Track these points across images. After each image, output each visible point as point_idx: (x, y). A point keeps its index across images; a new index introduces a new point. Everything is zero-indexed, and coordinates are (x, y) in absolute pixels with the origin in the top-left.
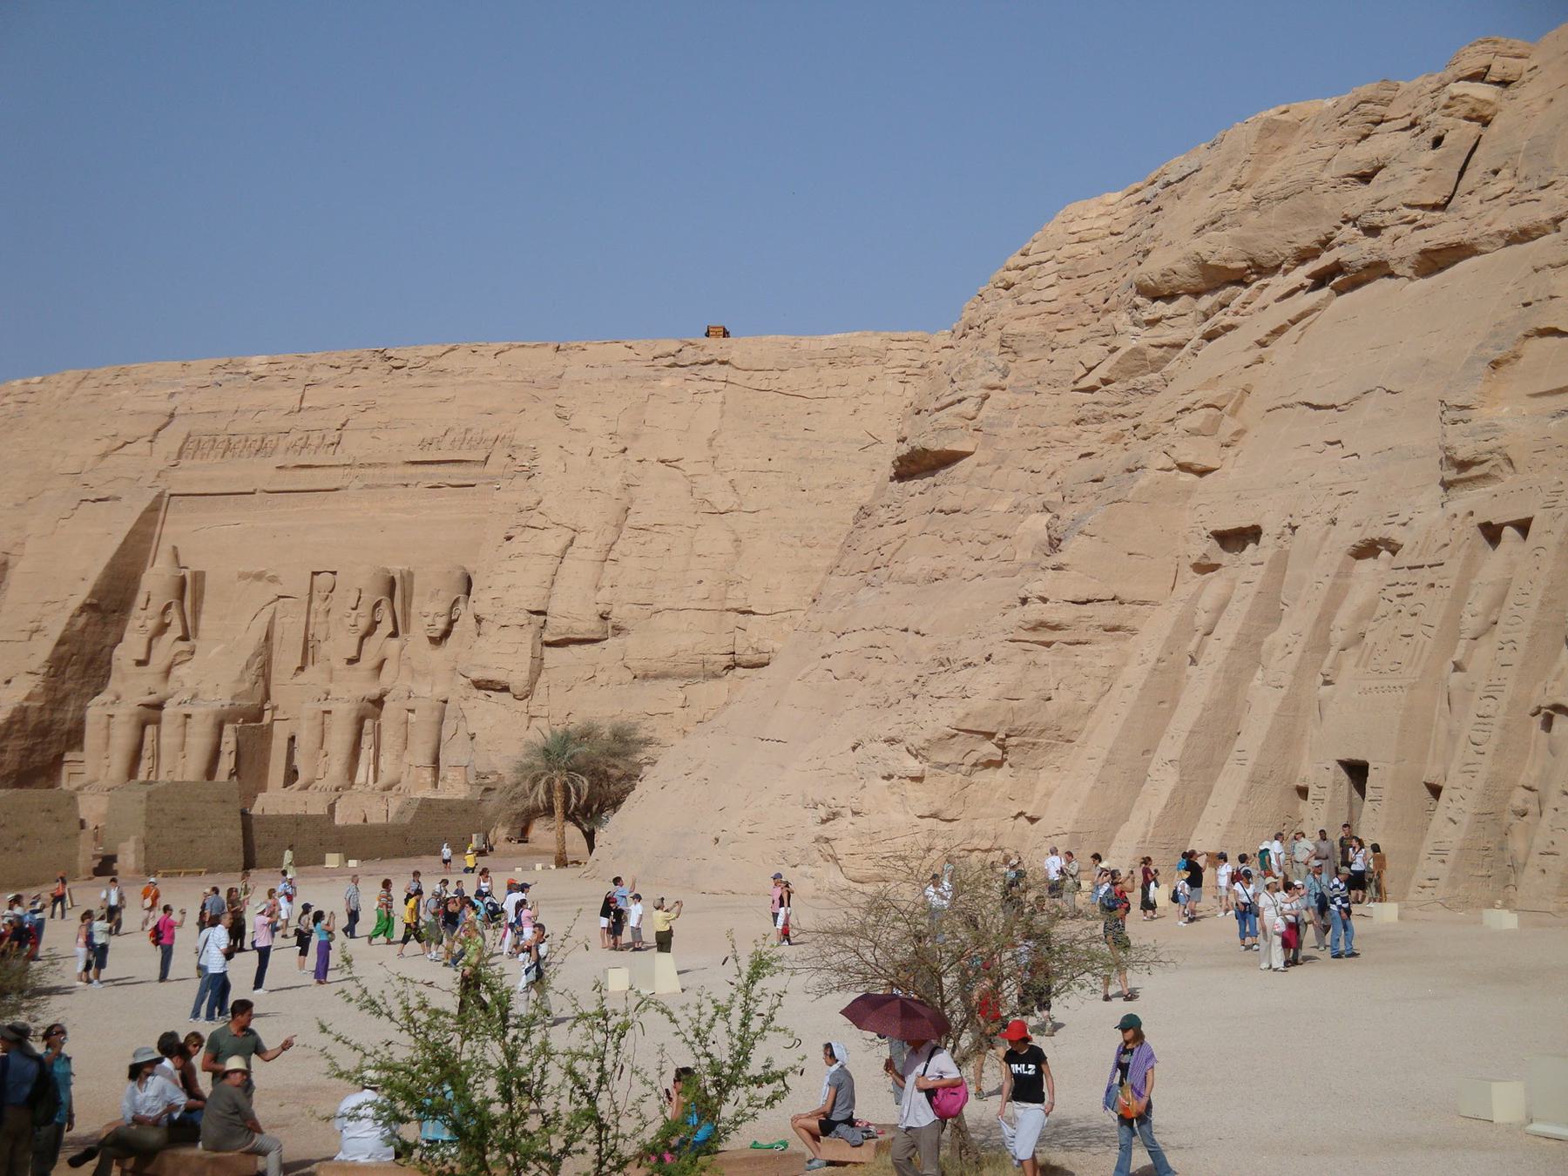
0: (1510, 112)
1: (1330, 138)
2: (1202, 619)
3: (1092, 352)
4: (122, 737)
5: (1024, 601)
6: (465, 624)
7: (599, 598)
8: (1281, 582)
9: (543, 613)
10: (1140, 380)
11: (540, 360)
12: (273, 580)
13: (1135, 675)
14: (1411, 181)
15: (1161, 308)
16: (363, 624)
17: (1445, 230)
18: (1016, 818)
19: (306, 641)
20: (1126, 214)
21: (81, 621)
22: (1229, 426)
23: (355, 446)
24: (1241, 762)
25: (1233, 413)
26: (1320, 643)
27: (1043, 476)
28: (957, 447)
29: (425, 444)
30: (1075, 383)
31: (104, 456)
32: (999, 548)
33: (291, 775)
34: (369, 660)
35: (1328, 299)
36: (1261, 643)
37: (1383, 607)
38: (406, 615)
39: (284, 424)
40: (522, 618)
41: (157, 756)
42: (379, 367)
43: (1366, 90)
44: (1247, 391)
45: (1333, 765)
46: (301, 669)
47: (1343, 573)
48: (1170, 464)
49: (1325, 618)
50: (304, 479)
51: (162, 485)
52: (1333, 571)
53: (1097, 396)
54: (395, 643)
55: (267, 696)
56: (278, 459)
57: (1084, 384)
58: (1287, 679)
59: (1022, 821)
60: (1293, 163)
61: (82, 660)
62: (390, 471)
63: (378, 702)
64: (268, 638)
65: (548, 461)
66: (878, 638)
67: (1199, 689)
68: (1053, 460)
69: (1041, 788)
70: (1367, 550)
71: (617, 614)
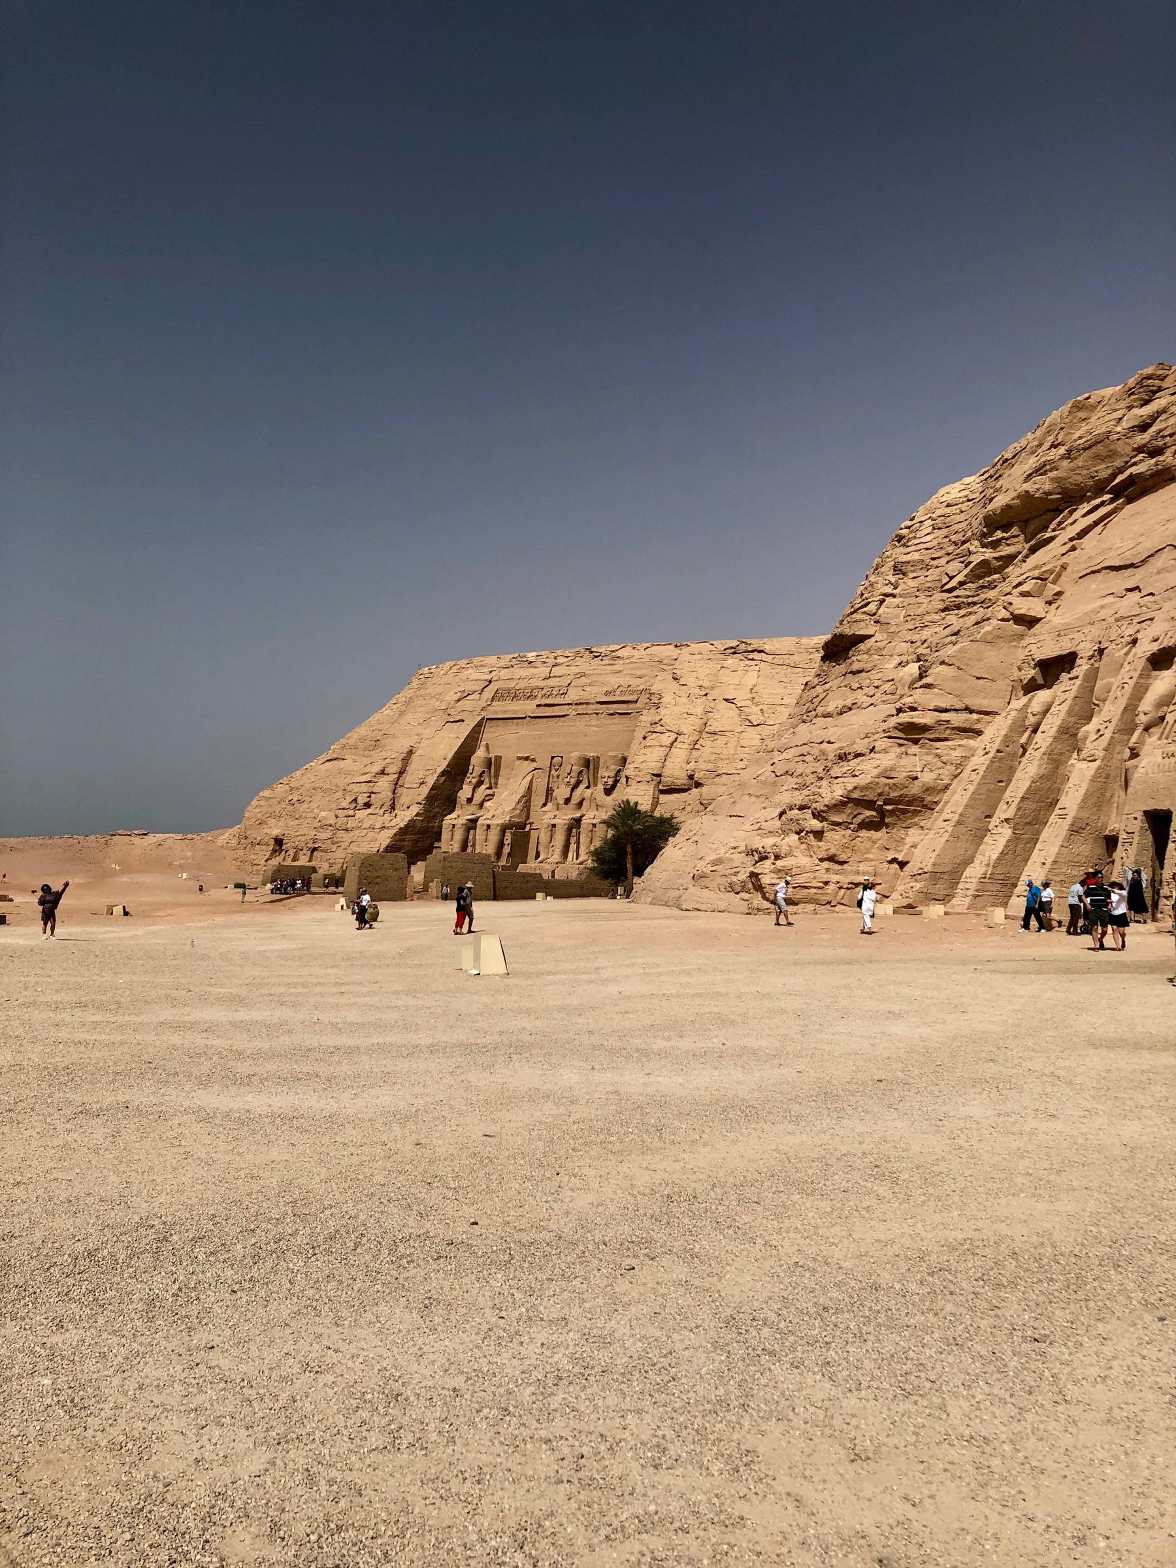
1: (1123, 404)
2: (1032, 720)
4: (459, 835)
6: (623, 780)
7: (688, 767)
8: (1092, 691)
9: (659, 775)
11: (669, 651)
12: (533, 760)
13: (980, 761)
16: (573, 781)
18: (890, 862)
19: (548, 790)
20: (979, 487)
22: (1052, 589)
23: (573, 695)
24: (1062, 817)
27: (919, 643)
28: (861, 632)
29: (607, 693)
30: (942, 586)
31: (459, 700)
32: (887, 687)
33: (538, 855)
34: (576, 798)
36: (1076, 735)
38: (595, 778)
39: (542, 684)
40: (649, 778)
41: (474, 845)
43: (1149, 370)
44: (1064, 567)
45: (1140, 815)
46: (544, 805)
48: (1008, 615)
49: (1131, 708)
50: (549, 711)
51: (484, 714)
52: (1136, 675)
53: (955, 593)
55: (528, 818)
56: (537, 702)
57: (946, 588)
58: (1100, 754)
59: (896, 866)
60: (1098, 424)
61: (443, 797)
62: (591, 707)
64: (530, 788)
65: (667, 699)
66: (805, 750)
67: (1028, 771)
68: (925, 634)
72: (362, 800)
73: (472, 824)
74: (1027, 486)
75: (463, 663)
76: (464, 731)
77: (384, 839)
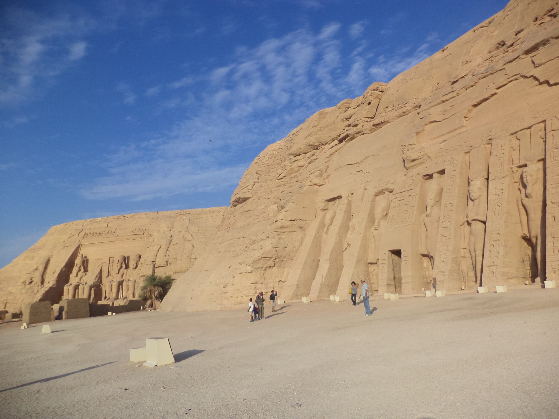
0: (384, 97)
2: (327, 222)
3: (280, 171)
5: (276, 221)
10: (293, 175)
14: (365, 112)
15: (298, 158)
16: (119, 266)
17: (377, 120)
21: (64, 269)
25: (325, 172)
26: (372, 219)
28: (248, 196)
33: (106, 297)
35: (345, 144)
37: (392, 205)
41: (78, 295)
42: (123, 218)
44: (328, 167)
45: (387, 252)
47: (374, 201)
54: (126, 270)
61: (63, 277)
63: (122, 282)
69: (285, 273)
70: (380, 193)
71: (170, 261)
72: (28, 281)
73: (77, 287)
74: (307, 141)
75: (71, 223)
76: (72, 250)
77: (39, 296)
